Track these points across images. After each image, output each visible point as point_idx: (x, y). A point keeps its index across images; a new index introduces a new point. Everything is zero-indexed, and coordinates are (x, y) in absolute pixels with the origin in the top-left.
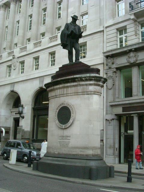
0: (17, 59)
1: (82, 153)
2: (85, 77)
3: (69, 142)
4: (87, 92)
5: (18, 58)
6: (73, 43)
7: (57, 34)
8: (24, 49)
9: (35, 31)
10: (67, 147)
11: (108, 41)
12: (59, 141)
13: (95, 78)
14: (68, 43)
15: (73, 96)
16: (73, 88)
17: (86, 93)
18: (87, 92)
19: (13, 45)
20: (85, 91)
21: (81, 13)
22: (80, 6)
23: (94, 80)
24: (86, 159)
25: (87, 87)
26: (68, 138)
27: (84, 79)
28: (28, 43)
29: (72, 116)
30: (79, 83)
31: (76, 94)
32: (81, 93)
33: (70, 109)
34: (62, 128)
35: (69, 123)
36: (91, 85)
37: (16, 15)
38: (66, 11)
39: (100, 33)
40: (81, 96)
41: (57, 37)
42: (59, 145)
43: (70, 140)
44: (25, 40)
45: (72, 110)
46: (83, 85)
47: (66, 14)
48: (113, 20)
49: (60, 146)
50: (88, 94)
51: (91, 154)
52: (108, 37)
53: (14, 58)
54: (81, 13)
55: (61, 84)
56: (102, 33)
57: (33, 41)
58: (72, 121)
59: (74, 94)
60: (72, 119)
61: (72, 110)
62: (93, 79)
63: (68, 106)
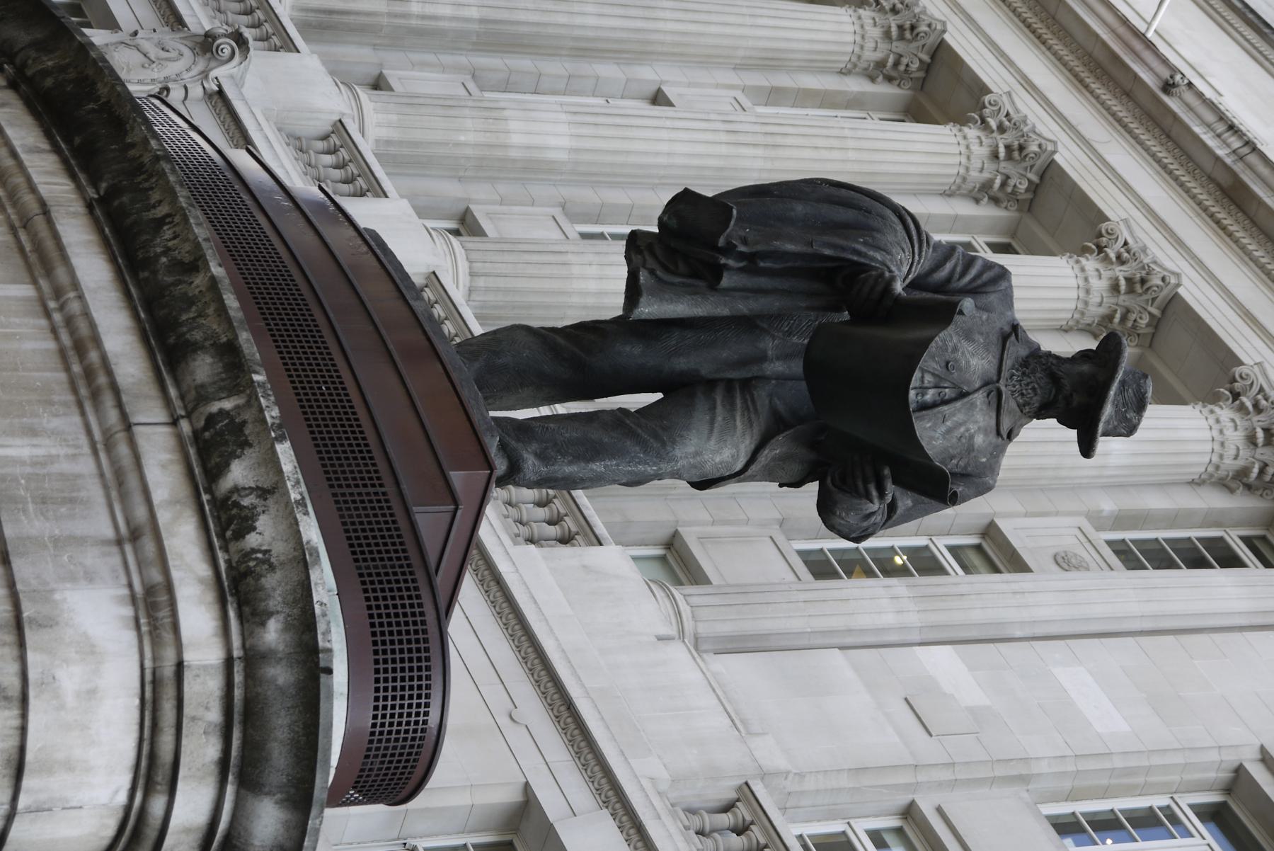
0: (196, 91)
2: (270, 491)
5: (219, 98)
6: (747, 385)
7: (601, 529)
8: (340, 166)
9: (592, 286)
13: (280, 675)
14: (726, 282)
19: (361, 56)
21: (939, 810)
22: (1023, 779)
23: (254, 659)
25: (106, 562)
27: (239, 473)
28: (431, 224)
37: (732, 78)
38: (913, 619)
41: (566, 540)
44: (451, 191)
47: (889, 619)
53: (206, 44)
54: (939, 810)
57: (463, 266)
62: (273, 634)
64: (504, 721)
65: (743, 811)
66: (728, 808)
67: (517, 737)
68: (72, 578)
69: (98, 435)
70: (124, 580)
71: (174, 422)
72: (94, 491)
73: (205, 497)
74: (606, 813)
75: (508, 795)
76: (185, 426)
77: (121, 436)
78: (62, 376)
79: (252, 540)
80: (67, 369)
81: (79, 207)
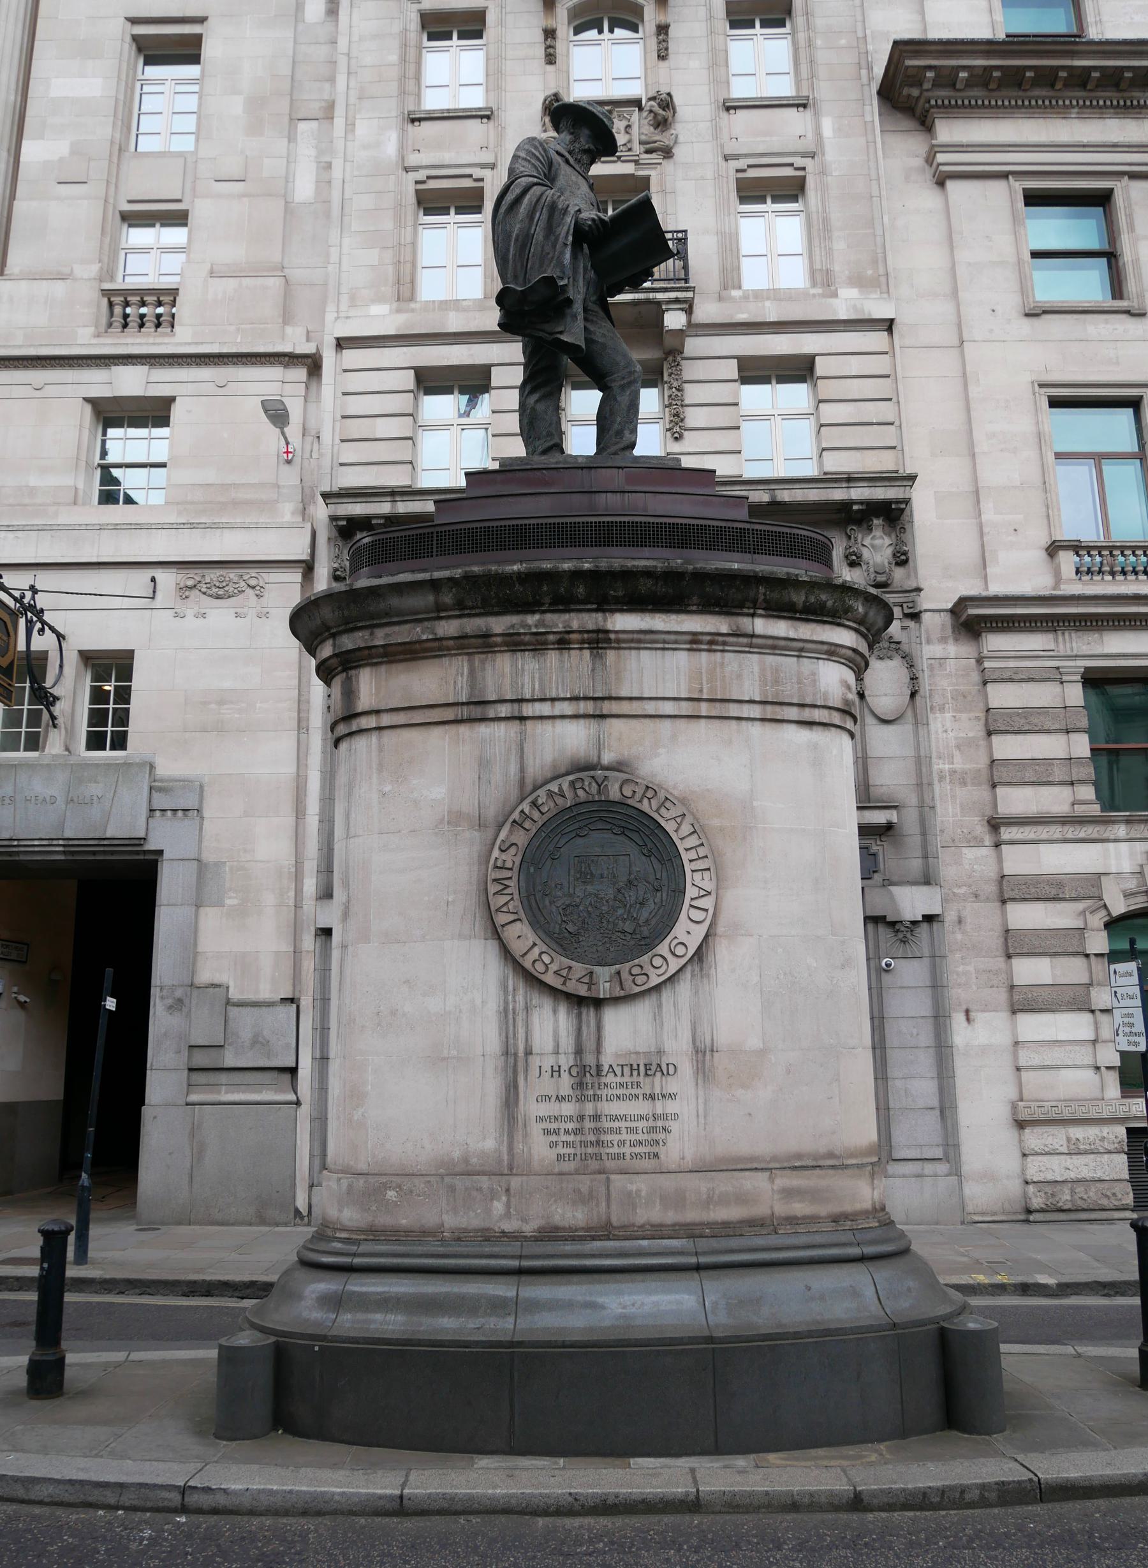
1: (800, 1208)
3: (665, 1117)
4: (802, 706)
10: (646, 1164)
11: (357, 428)
12: (540, 1119)
15: (681, 724)
16: (681, 659)
17: (793, 713)
18: (802, 706)
20: (790, 692)
21: (130, 202)
24: (855, 1251)
25: (807, 665)
26: (657, 1084)
29: (691, 892)
30: (745, 623)
31: (704, 709)
32: (755, 711)
33: (670, 827)
34: (583, 991)
35: (663, 948)
36: (832, 652)
39: (286, 366)
40: (756, 730)
42: (551, 1154)
43: (672, 1096)
45: (693, 841)
46: (775, 646)
48: (398, 311)
49: (560, 1157)
50: (810, 724)
51: (867, 1205)
52: (356, 405)
54: (130, 202)
55: (564, 603)
56: (301, 373)
58: (700, 932)
59: (685, 708)
60: (697, 915)
61: (693, 841)
63: (645, 806)
64: (38, 394)
65: (117, 299)
66: (111, 305)
67: (49, 391)
68: (814, 681)
69: (747, 649)
70: (816, 660)
71: (753, 615)
72: (771, 660)
73: (798, 615)
74: (113, 368)
75: (88, 409)
76: (760, 612)
77: (755, 641)
78: (704, 654)
79: (830, 603)
80: (700, 650)
81: (600, 616)
